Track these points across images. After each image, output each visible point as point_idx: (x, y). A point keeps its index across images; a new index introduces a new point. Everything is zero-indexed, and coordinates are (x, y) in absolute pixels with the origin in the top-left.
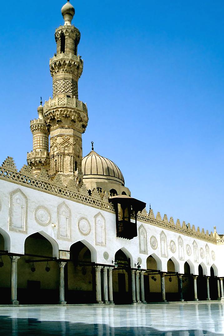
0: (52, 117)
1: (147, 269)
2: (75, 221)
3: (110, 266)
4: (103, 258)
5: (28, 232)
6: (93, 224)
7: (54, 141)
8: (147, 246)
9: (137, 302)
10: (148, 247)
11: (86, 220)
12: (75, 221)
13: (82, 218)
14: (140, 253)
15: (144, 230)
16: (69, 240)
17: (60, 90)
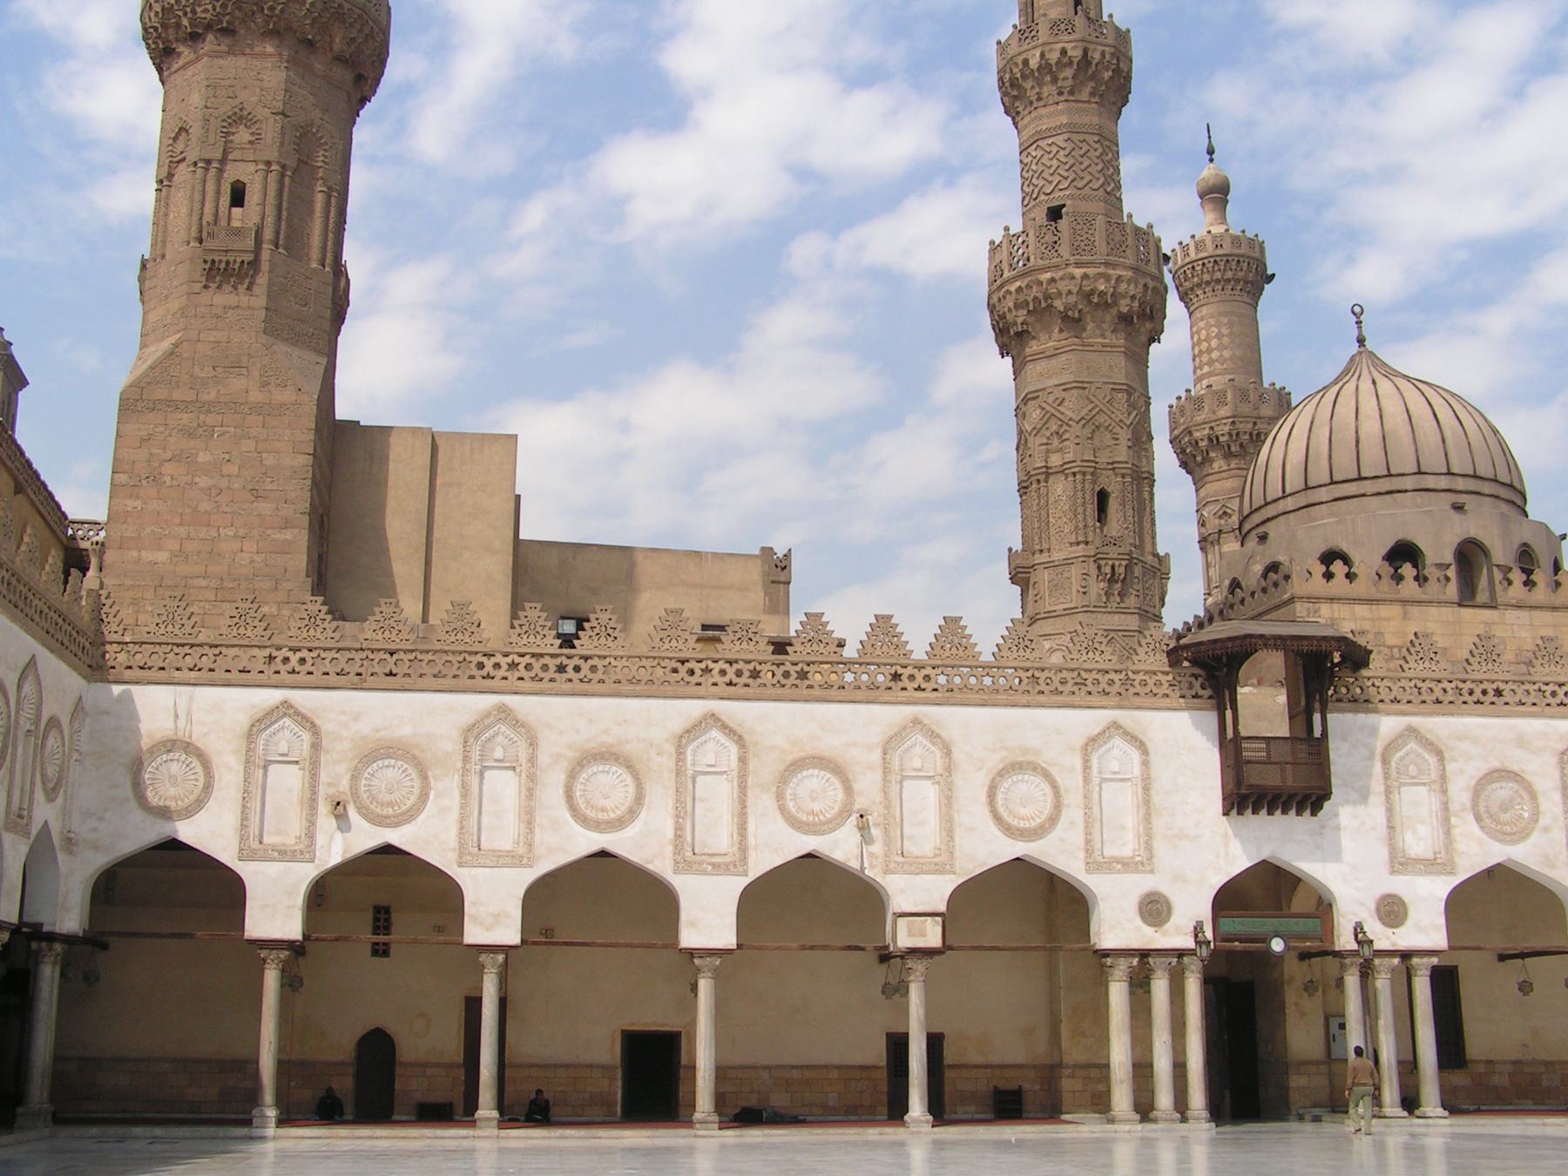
0: (1044, 305)
1: (1451, 948)
2: (971, 789)
3: (1180, 953)
4: (1139, 922)
5: (751, 865)
6: (1071, 782)
7: (1048, 408)
8: (1448, 832)
9: (1410, 1103)
10: (1456, 832)
11: (1034, 769)
12: (971, 789)
13: (1014, 768)
14: (1393, 872)
15: (1427, 756)
16: (940, 869)
17: (1057, 179)
